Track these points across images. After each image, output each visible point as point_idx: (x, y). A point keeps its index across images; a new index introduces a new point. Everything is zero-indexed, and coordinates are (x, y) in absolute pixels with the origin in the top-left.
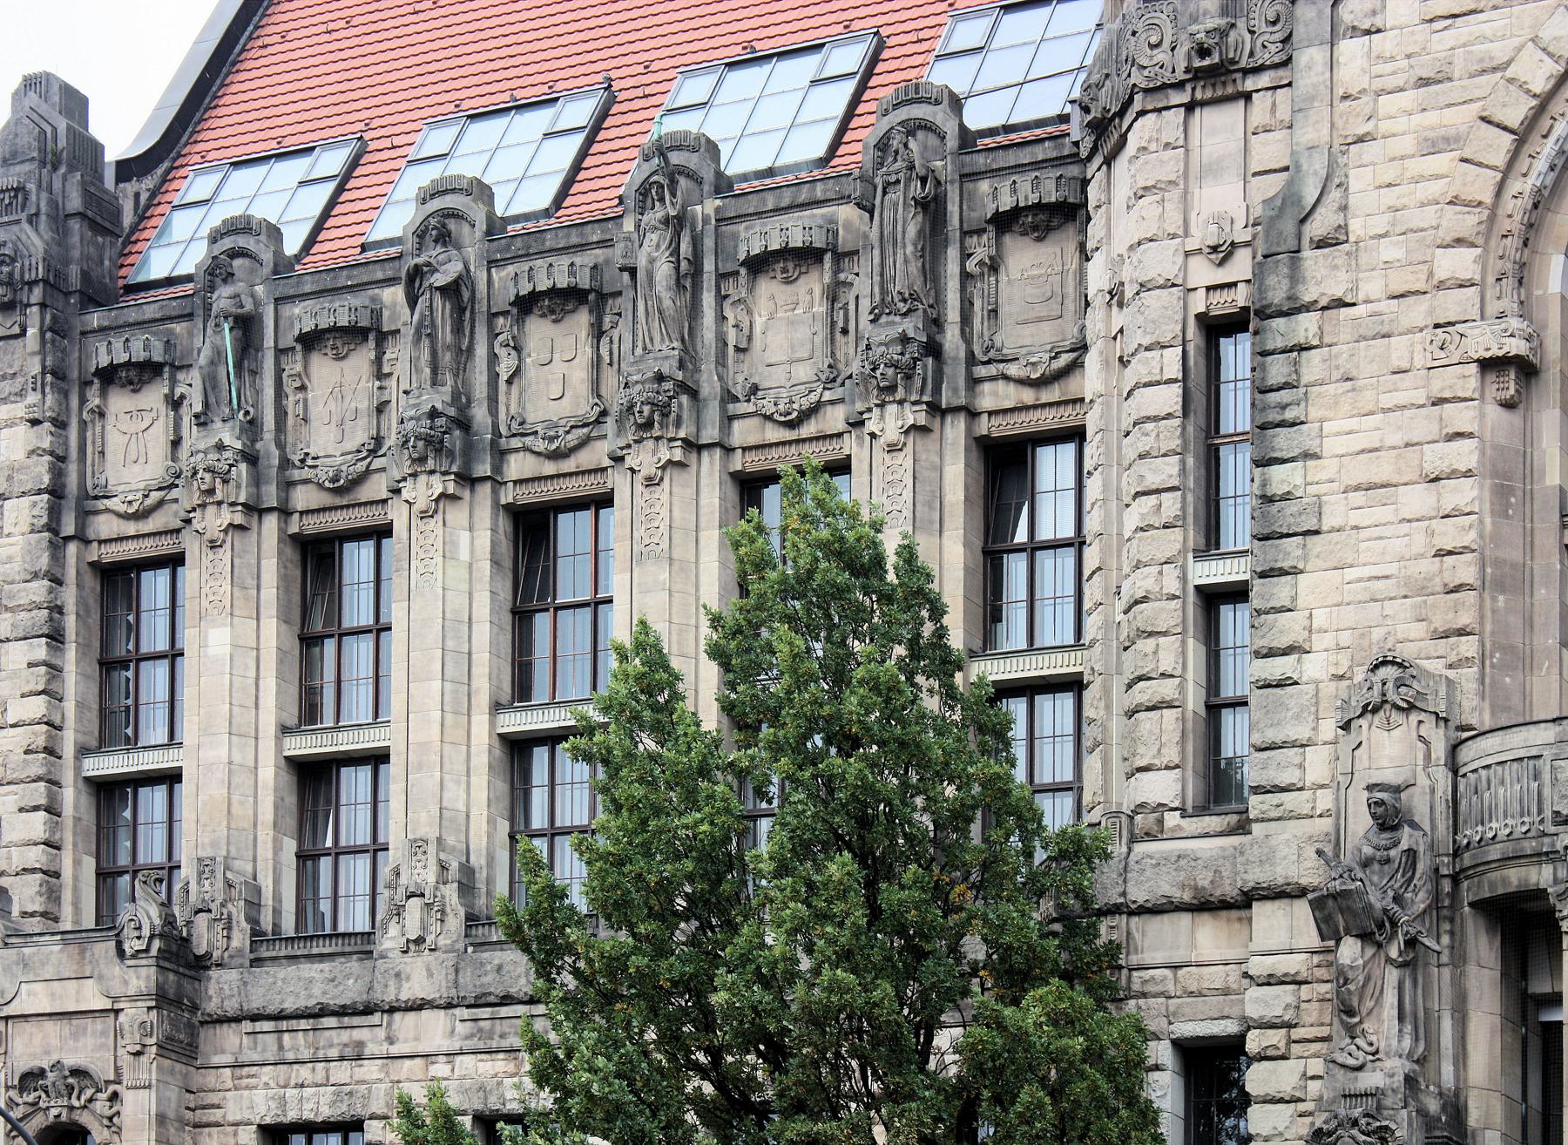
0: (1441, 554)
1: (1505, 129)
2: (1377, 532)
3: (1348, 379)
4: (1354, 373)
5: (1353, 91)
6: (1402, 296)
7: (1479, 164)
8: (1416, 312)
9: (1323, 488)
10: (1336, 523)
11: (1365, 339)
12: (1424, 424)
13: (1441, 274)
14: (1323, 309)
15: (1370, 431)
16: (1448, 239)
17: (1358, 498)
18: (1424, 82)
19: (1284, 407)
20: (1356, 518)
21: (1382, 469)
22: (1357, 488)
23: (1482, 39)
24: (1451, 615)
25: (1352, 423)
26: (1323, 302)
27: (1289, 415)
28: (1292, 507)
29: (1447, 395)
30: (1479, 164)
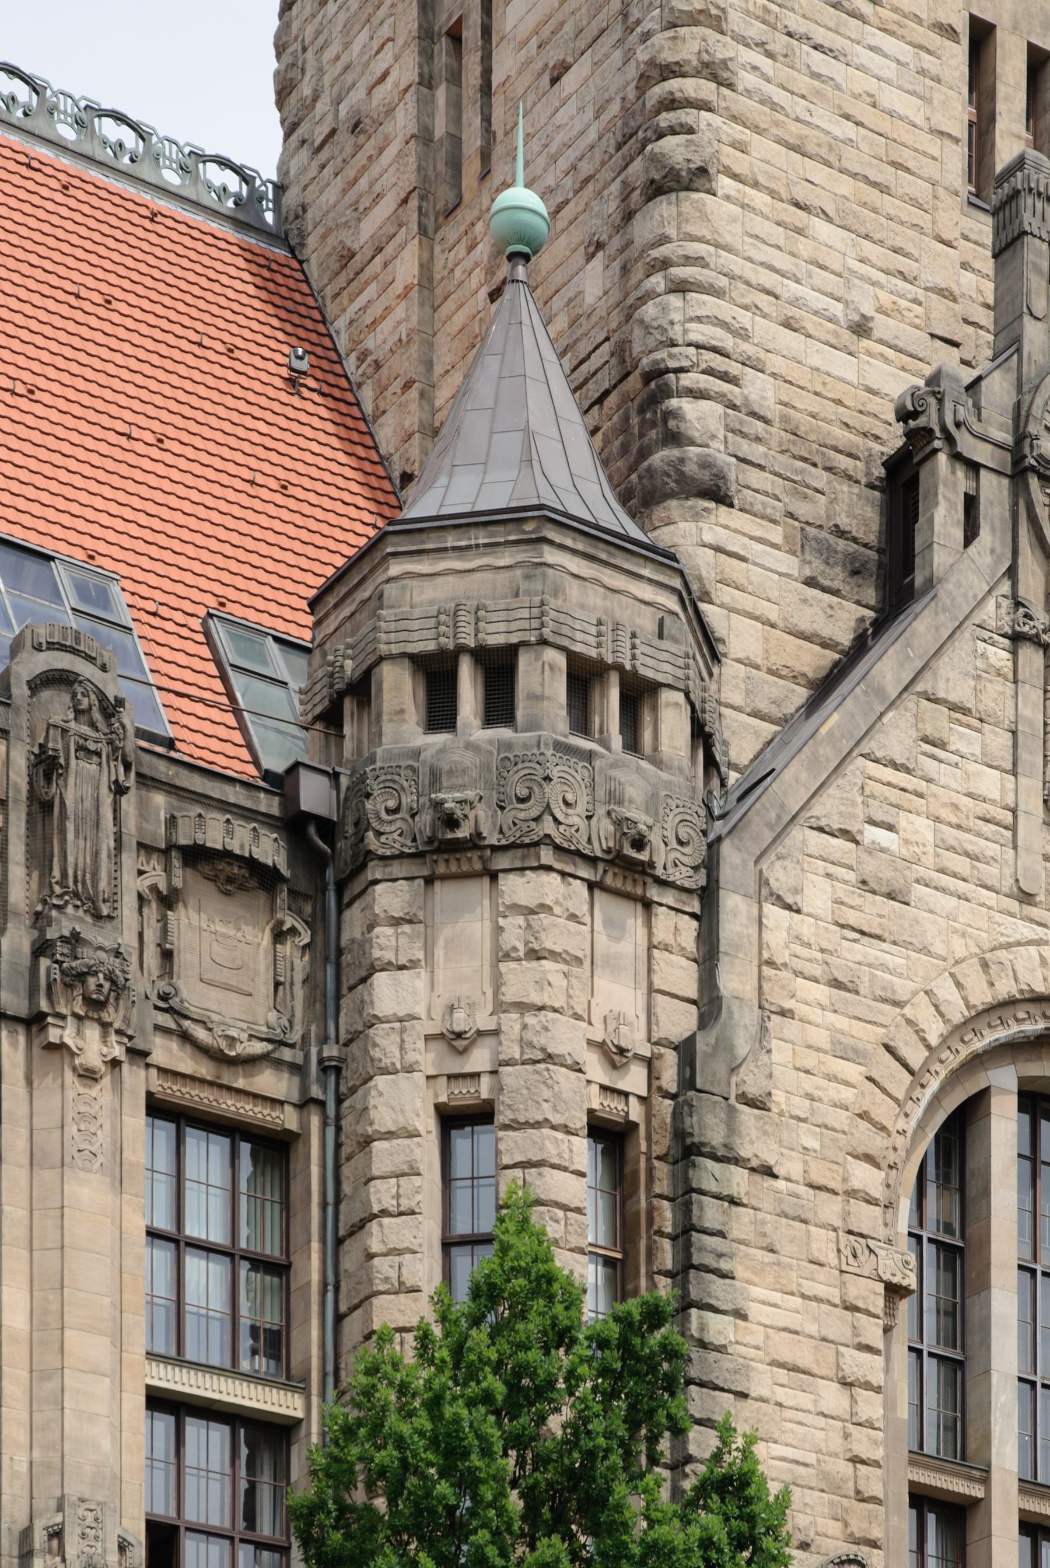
0: (856, 1460)
1: (906, 1066)
2: (800, 1416)
3: (772, 1251)
4: (777, 1247)
5: (779, 961)
6: (819, 1188)
7: (884, 1091)
8: (830, 1209)
9: (752, 1353)
10: (765, 1393)
11: (786, 1216)
12: (838, 1325)
13: (856, 1183)
14: (753, 1170)
15: (790, 1312)
16: (860, 1150)
17: (782, 1374)
18: (836, 984)
19: (720, 1256)
20: (780, 1395)
21: (802, 1354)
22: (782, 1365)
23: (884, 967)
24: (865, 1525)
25: (776, 1297)
26: (754, 1163)
27: (724, 1265)
28: (726, 1363)
29: (860, 1304)
30: (884, 1091)
